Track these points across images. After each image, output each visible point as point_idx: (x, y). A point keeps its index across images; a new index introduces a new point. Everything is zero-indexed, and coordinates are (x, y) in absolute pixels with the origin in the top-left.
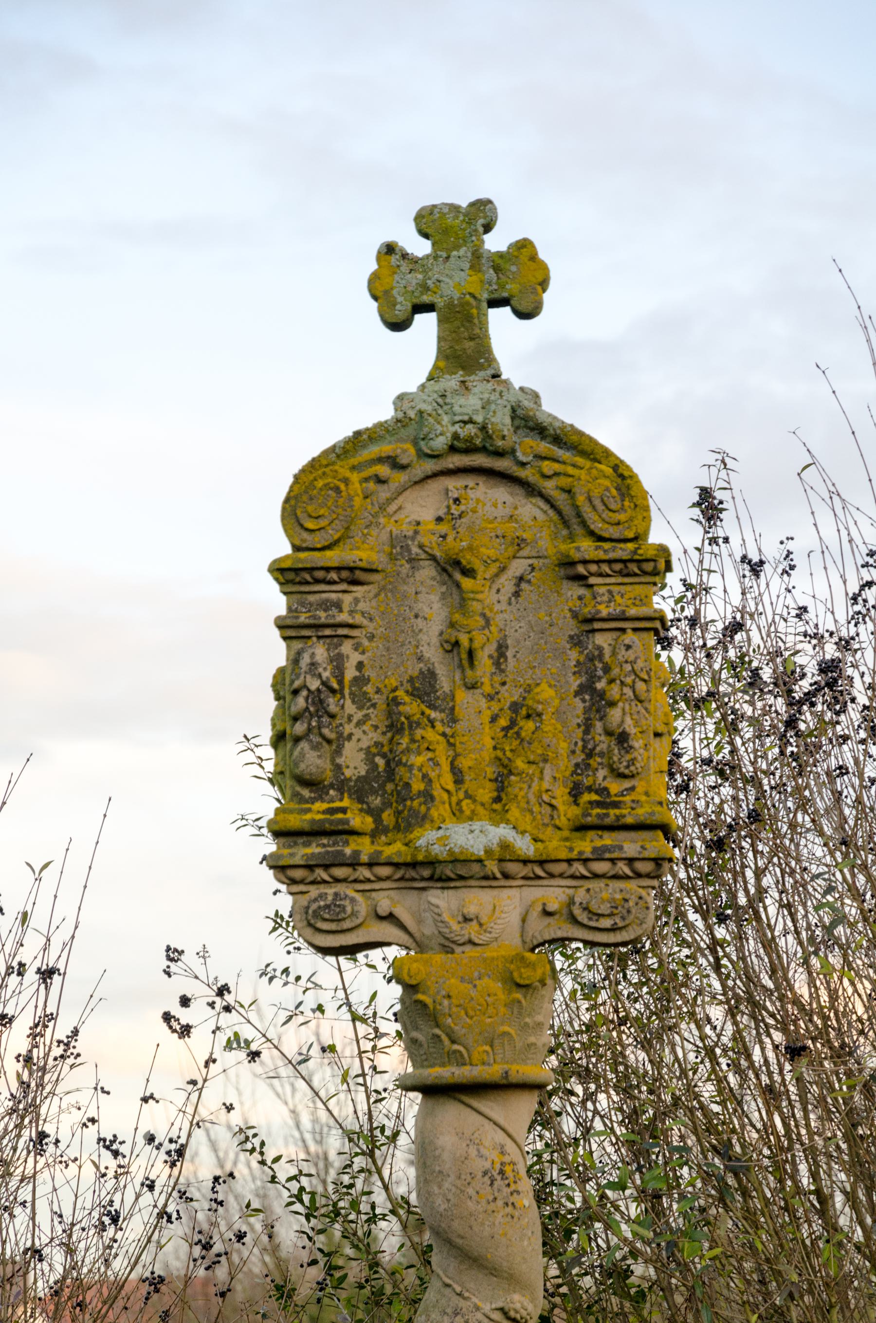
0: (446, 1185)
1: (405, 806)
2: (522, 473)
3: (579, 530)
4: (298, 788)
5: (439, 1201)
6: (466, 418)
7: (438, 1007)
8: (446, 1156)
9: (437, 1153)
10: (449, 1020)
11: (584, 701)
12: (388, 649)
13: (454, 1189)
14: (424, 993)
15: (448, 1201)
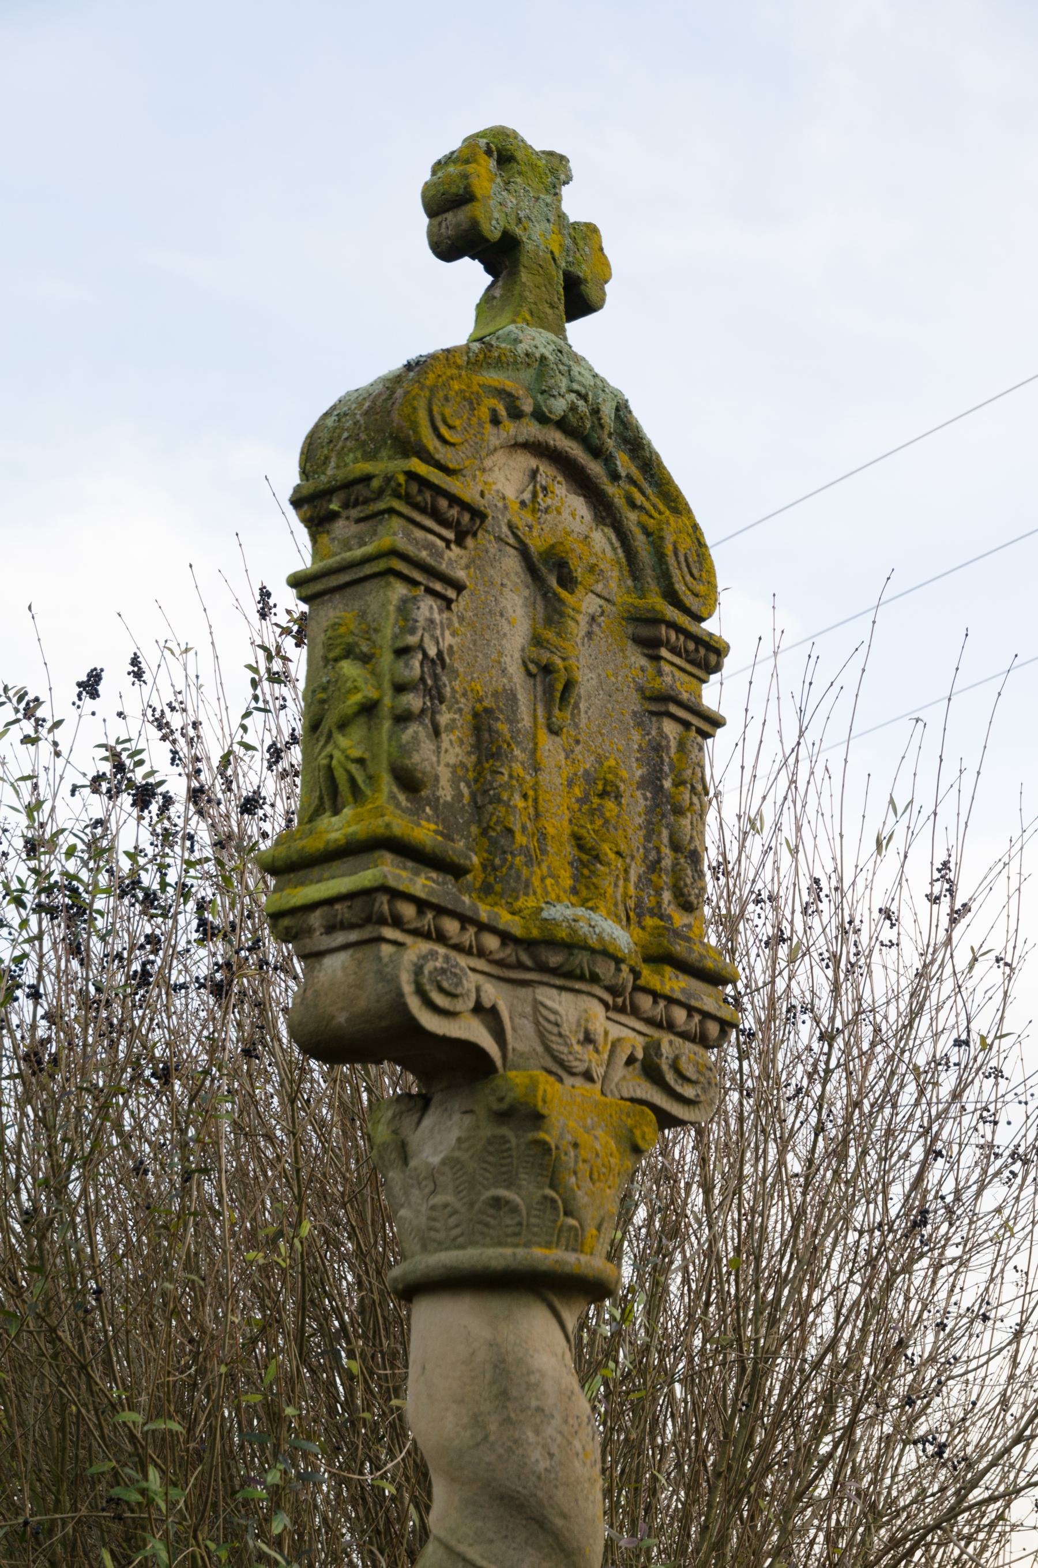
0: (550, 1431)
1: (505, 860)
2: (612, 490)
3: (653, 587)
4: (395, 790)
5: (536, 1454)
6: (583, 391)
7: (563, 1157)
8: (548, 1386)
9: (533, 1379)
10: (573, 1179)
11: (646, 799)
12: (475, 643)
13: (559, 1439)
14: (547, 1132)
15: (551, 1455)
